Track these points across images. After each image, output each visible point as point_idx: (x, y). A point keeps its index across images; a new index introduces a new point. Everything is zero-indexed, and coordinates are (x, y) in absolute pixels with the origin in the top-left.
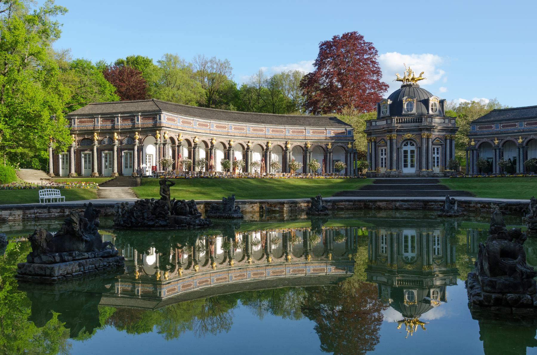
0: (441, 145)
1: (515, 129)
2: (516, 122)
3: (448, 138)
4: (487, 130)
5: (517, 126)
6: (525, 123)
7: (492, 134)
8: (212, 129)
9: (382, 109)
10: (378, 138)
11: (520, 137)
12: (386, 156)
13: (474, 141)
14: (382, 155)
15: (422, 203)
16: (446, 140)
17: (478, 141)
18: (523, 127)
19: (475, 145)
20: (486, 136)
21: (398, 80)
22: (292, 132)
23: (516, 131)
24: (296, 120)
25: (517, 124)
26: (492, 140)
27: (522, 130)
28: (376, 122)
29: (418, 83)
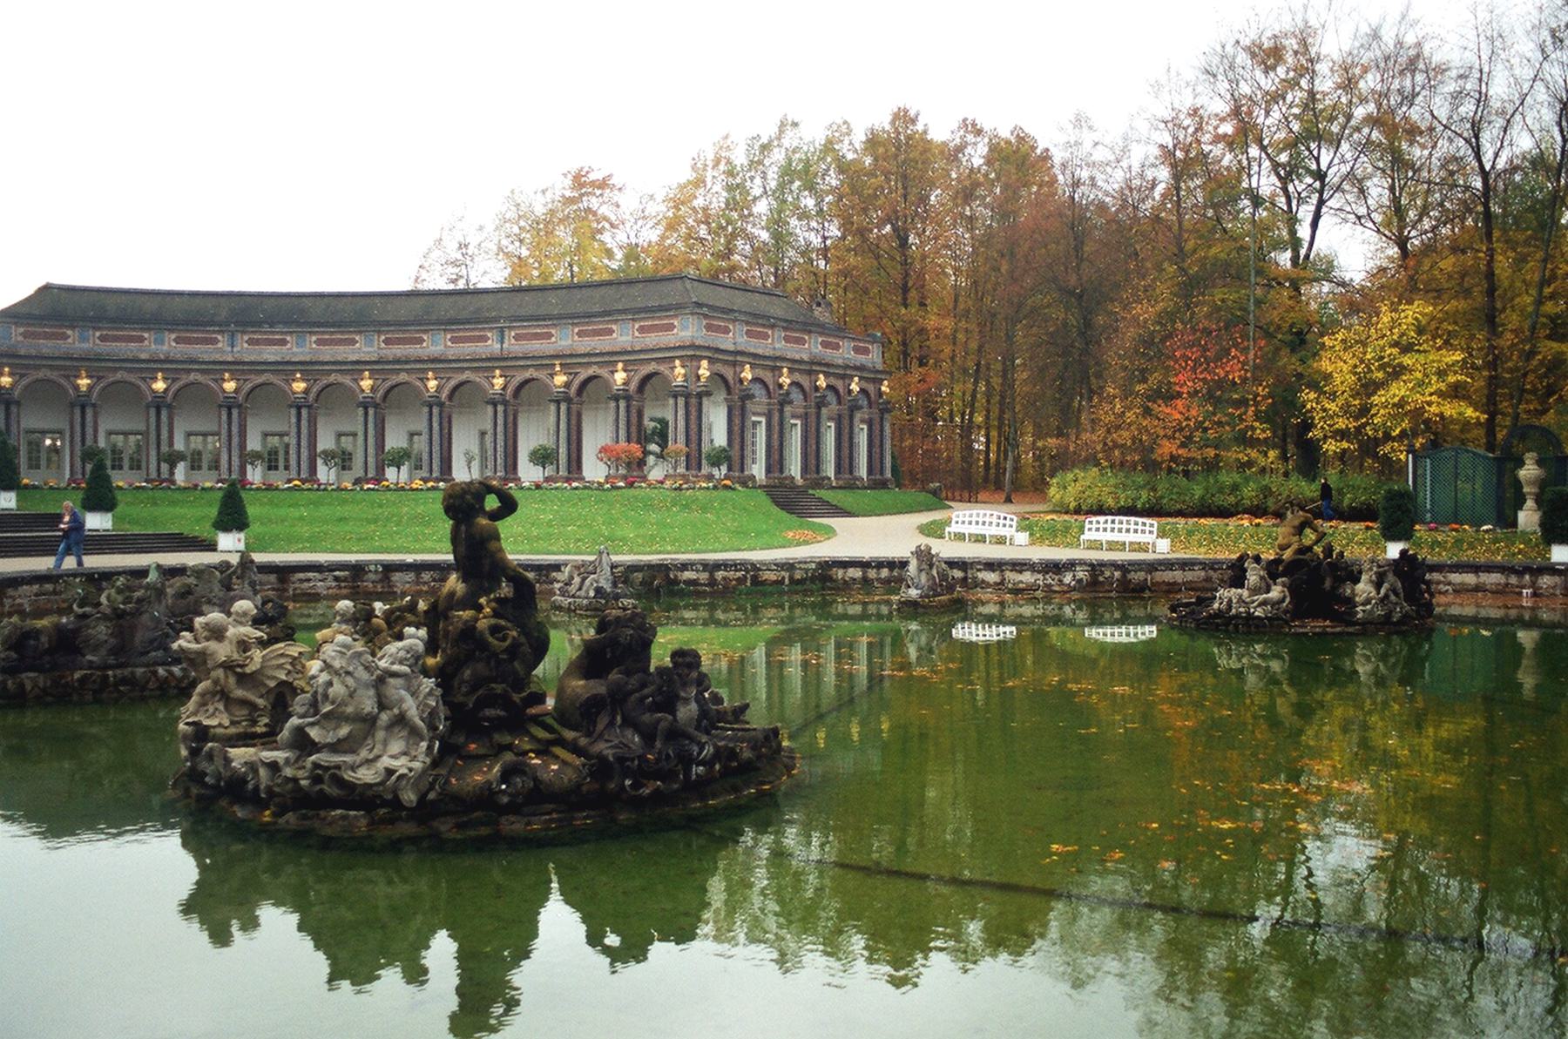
1: (142, 351)
2: (142, 330)
4: (50, 343)
5: (146, 342)
6: (173, 336)
7: (72, 359)
11: (160, 375)
15: (273, 578)
17: (22, 376)
18: (165, 348)
20: (50, 363)
23: (143, 356)
25: (146, 335)
26: (67, 377)
27: (162, 357)
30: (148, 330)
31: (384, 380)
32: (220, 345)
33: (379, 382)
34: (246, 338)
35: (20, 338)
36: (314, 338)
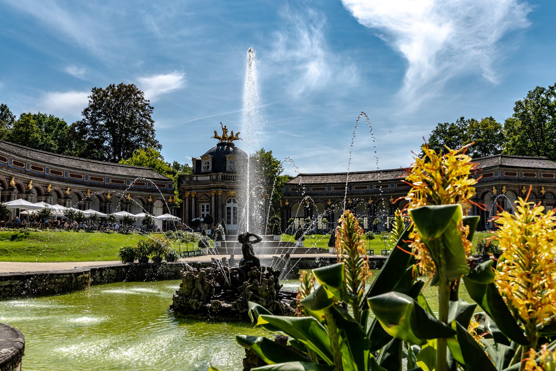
6: (333, 188)
8: (28, 170)
9: (203, 165)
10: (199, 194)
12: (208, 213)
14: (203, 211)
17: (291, 201)
19: (289, 205)
21: (216, 137)
22: (112, 181)
24: (113, 168)
28: (197, 177)
29: (234, 142)
35: (291, 191)
36: (375, 186)
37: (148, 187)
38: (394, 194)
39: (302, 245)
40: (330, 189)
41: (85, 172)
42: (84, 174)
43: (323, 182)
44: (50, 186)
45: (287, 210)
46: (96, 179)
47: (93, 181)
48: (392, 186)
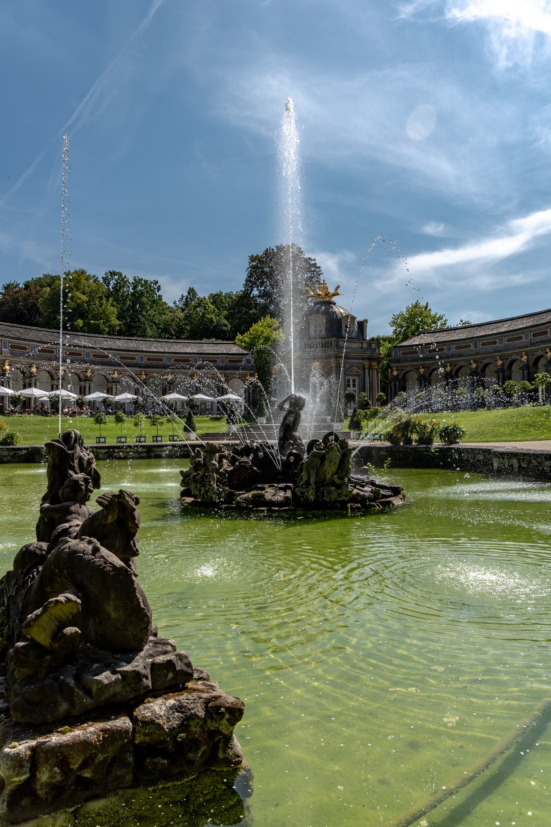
0: (358, 376)
3: (367, 366)
5: (445, 351)
6: (454, 347)
11: (448, 365)
13: (397, 370)
16: (364, 369)
17: (402, 370)
29: (334, 299)
30: (445, 345)
31: (533, 355)
32: (471, 348)
33: (530, 357)
34: (481, 343)
35: (401, 355)
36: (506, 339)
37: (221, 364)
38: (528, 349)
39: (340, 428)
40: (449, 349)
41: (138, 353)
42: (137, 355)
43: (443, 339)
44: (89, 370)
45: (395, 382)
46: (155, 360)
47: (150, 362)
48: (527, 336)
